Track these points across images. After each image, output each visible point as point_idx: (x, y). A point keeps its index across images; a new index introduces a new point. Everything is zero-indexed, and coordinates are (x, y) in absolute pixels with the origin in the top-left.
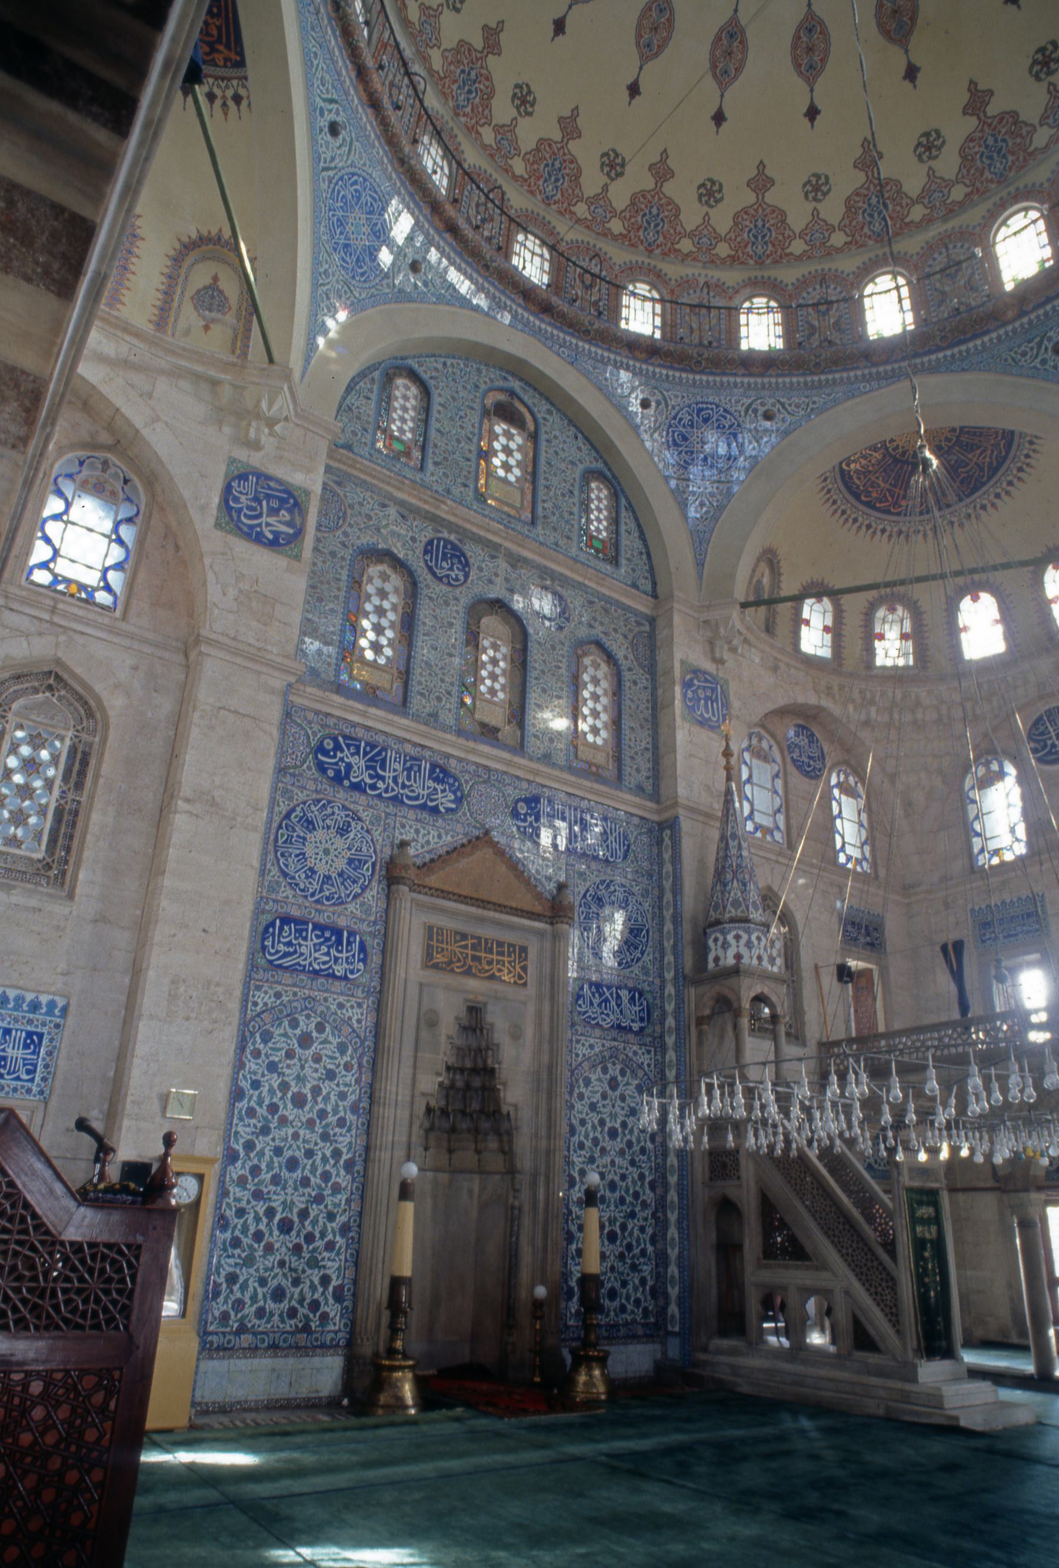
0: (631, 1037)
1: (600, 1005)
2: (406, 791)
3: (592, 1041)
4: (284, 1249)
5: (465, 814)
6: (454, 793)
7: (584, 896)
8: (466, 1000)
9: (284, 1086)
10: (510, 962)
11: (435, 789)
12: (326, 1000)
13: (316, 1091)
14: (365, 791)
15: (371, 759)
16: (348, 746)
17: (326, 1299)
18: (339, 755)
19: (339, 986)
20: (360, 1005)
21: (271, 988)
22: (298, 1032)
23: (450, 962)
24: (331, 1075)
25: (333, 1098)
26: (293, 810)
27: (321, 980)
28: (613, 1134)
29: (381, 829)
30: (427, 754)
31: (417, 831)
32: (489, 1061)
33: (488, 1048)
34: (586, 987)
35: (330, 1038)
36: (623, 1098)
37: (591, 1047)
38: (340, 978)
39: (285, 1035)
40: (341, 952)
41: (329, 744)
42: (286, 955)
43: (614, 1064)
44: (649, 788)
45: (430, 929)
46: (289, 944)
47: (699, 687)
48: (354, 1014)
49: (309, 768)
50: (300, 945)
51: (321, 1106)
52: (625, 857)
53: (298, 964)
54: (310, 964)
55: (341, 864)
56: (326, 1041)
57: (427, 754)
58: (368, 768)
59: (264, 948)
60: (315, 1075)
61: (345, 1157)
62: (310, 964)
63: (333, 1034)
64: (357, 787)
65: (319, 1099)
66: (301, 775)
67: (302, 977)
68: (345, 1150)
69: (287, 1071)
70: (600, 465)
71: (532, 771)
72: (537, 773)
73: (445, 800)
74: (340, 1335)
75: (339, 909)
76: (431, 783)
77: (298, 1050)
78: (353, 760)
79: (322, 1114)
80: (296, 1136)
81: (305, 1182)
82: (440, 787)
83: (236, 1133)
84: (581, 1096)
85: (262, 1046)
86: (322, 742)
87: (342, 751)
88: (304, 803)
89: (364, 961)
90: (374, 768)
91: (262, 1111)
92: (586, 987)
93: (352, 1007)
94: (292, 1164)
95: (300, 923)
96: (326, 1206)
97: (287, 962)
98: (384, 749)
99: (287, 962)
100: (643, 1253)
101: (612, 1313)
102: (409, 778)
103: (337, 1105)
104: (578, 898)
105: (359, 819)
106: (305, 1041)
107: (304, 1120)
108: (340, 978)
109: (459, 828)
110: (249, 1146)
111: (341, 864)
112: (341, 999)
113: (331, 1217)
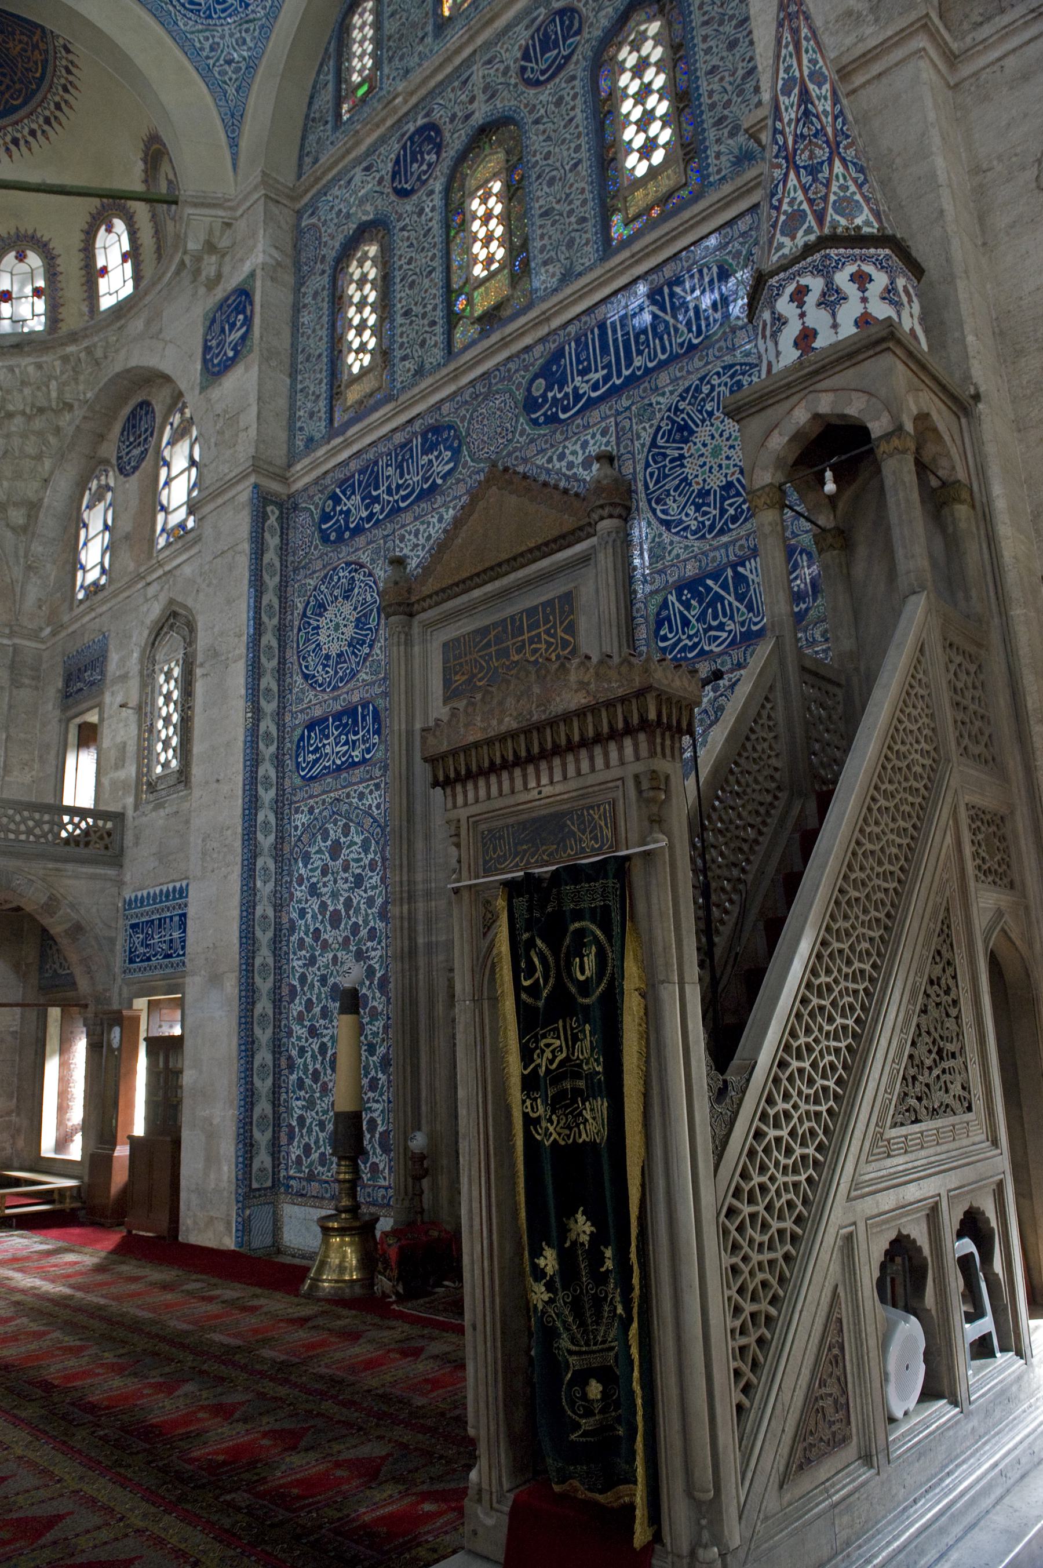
1: (701, 618)
7: (654, 444)
9: (323, 906)
10: (547, 632)
12: (348, 796)
14: (364, 529)
15: (368, 485)
16: (344, 493)
19: (358, 773)
20: (377, 786)
22: (329, 843)
25: (363, 907)
30: (417, 426)
34: (672, 598)
35: (356, 839)
38: (359, 763)
40: (356, 733)
50: (324, 745)
51: (354, 919)
53: (325, 768)
55: (349, 631)
56: (353, 843)
58: (363, 500)
59: (298, 764)
60: (346, 886)
61: (378, 975)
63: (357, 833)
64: (358, 531)
68: (377, 966)
69: (324, 890)
71: (537, 323)
75: (350, 686)
77: (331, 863)
79: (355, 929)
86: (323, 510)
89: (378, 732)
90: (369, 495)
91: (308, 940)
98: (376, 463)
99: (315, 772)
102: (402, 476)
103: (367, 915)
104: (641, 457)
105: (362, 566)
106: (335, 850)
108: (359, 763)
110: (303, 978)
111: (349, 631)
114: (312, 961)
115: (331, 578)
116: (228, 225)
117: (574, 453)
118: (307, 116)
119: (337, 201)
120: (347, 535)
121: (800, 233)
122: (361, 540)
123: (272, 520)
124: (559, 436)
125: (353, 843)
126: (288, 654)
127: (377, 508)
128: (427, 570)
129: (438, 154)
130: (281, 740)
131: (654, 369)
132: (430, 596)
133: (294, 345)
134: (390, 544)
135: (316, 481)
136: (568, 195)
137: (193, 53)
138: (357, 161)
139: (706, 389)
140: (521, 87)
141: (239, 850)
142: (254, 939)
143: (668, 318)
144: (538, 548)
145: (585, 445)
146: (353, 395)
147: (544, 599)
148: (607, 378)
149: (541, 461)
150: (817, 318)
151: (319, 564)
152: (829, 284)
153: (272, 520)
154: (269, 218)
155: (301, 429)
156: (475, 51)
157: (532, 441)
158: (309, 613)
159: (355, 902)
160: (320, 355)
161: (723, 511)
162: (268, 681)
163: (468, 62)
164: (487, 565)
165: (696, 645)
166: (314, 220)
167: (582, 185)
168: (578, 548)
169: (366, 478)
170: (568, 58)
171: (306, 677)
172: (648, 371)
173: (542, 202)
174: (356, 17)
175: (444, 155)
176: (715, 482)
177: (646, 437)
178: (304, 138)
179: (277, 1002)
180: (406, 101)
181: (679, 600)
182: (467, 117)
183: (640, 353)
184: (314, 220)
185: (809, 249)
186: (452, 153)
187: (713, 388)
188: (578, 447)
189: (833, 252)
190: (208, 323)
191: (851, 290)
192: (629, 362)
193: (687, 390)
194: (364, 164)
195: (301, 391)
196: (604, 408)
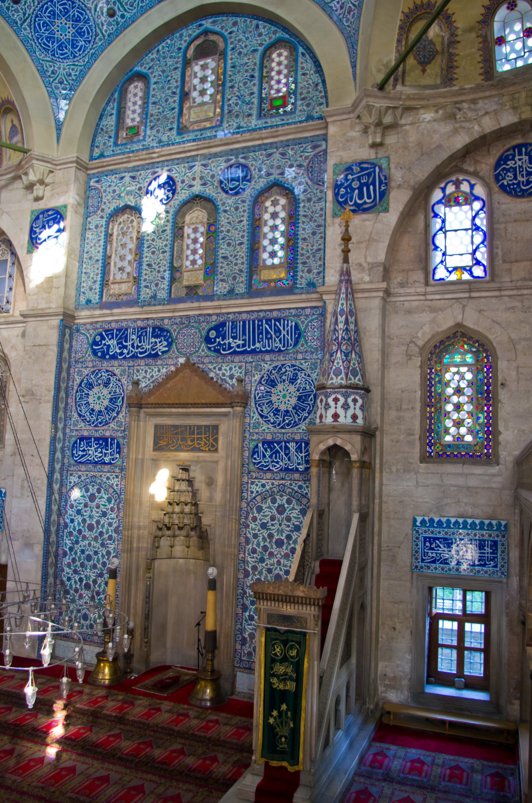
0: (296, 476)
1: (271, 457)
2: (139, 350)
3: (264, 482)
5: (174, 352)
6: (167, 340)
9: (84, 521)
10: (206, 438)
11: (156, 342)
12: (101, 476)
13: (98, 522)
15: (121, 338)
16: (107, 336)
19: (107, 468)
20: (117, 477)
23: (168, 444)
24: (104, 514)
25: (106, 526)
26: (83, 381)
27: (99, 466)
28: (279, 543)
29: (126, 377)
30: (150, 322)
31: (146, 372)
34: (260, 445)
36: (289, 519)
37: (263, 486)
40: (107, 450)
41: (98, 338)
42: (83, 456)
43: (282, 496)
45: (156, 426)
46: (84, 450)
47: (353, 180)
52: (296, 344)
55: (106, 403)
56: (102, 497)
57: (150, 322)
58: (118, 344)
59: (73, 454)
64: (114, 357)
67: (90, 466)
70: (280, 34)
71: (216, 308)
72: (220, 307)
75: (106, 427)
76: (153, 340)
77: (89, 503)
80: (90, 544)
81: (95, 567)
84: (255, 519)
86: (94, 339)
89: (119, 453)
90: (121, 343)
91: (75, 533)
94: (89, 558)
95: (88, 438)
99: (83, 460)
102: (140, 342)
105: (115, 375)
109: (170, 362)
114: (77, 542)
115: (97, 374)
116: (51, 172)
117: (226, 370)
118: (98, 125)
119: (113, 184)
120: (107, 357)
121: (339, 378)
122: (116, 363)
123: (67, 336)
124: (219, 360)
125: (102, 497)
126: (70, 401)
127: (125, 351)
128: (151, 392)
129: (173, 194)
130: (64, 440)
131: (264, 352)
133: (82, 246)
134: (131, 371)
135: (91, 323)
136: (236, 256)
137: (43, 73)
138: (128, 170)
139: (284, 370)
140: (220, 190)
142: (50, 531)
143: (272, 333)
145: (231, 369)
146: (115, 289)
148: (244, 345)
149: (211, 366)
150: (341, 412)
151: (90, 364)
152: (346, 401)
153: (67, 336)
154: (77, 179)
155: (84, 293)
156: (197, 155)
157: (207, 356)
158: (83, 385)
160: (97, 261)
161: (284, 420)
162: (61, 414)
163: (194, 158)
164: (181, 402)
166: (98, 186)
167: (243, 255)
168: (223, 410)
169: (121, 334)
171: (80, 415)
172: (261, 351)
173: (223, 251)
174: (132, 86)
175: (176, 197)
176: (283, 408)
178: (95, 136)
179: (56, 556)
181: (263, 446)
182: (191, 186)
183: (259, 342)
184: (98, 186)
185: (341, 387)
186: (181, 199)
187: (286, 371)
188: (228, 368)
189: (349, 390)
190: (34, 217)
191: (351, 404)
192: (254, 344)
193: (276, 367)
194: (131, 174)
195: (85, 273)
196: (241, 357)
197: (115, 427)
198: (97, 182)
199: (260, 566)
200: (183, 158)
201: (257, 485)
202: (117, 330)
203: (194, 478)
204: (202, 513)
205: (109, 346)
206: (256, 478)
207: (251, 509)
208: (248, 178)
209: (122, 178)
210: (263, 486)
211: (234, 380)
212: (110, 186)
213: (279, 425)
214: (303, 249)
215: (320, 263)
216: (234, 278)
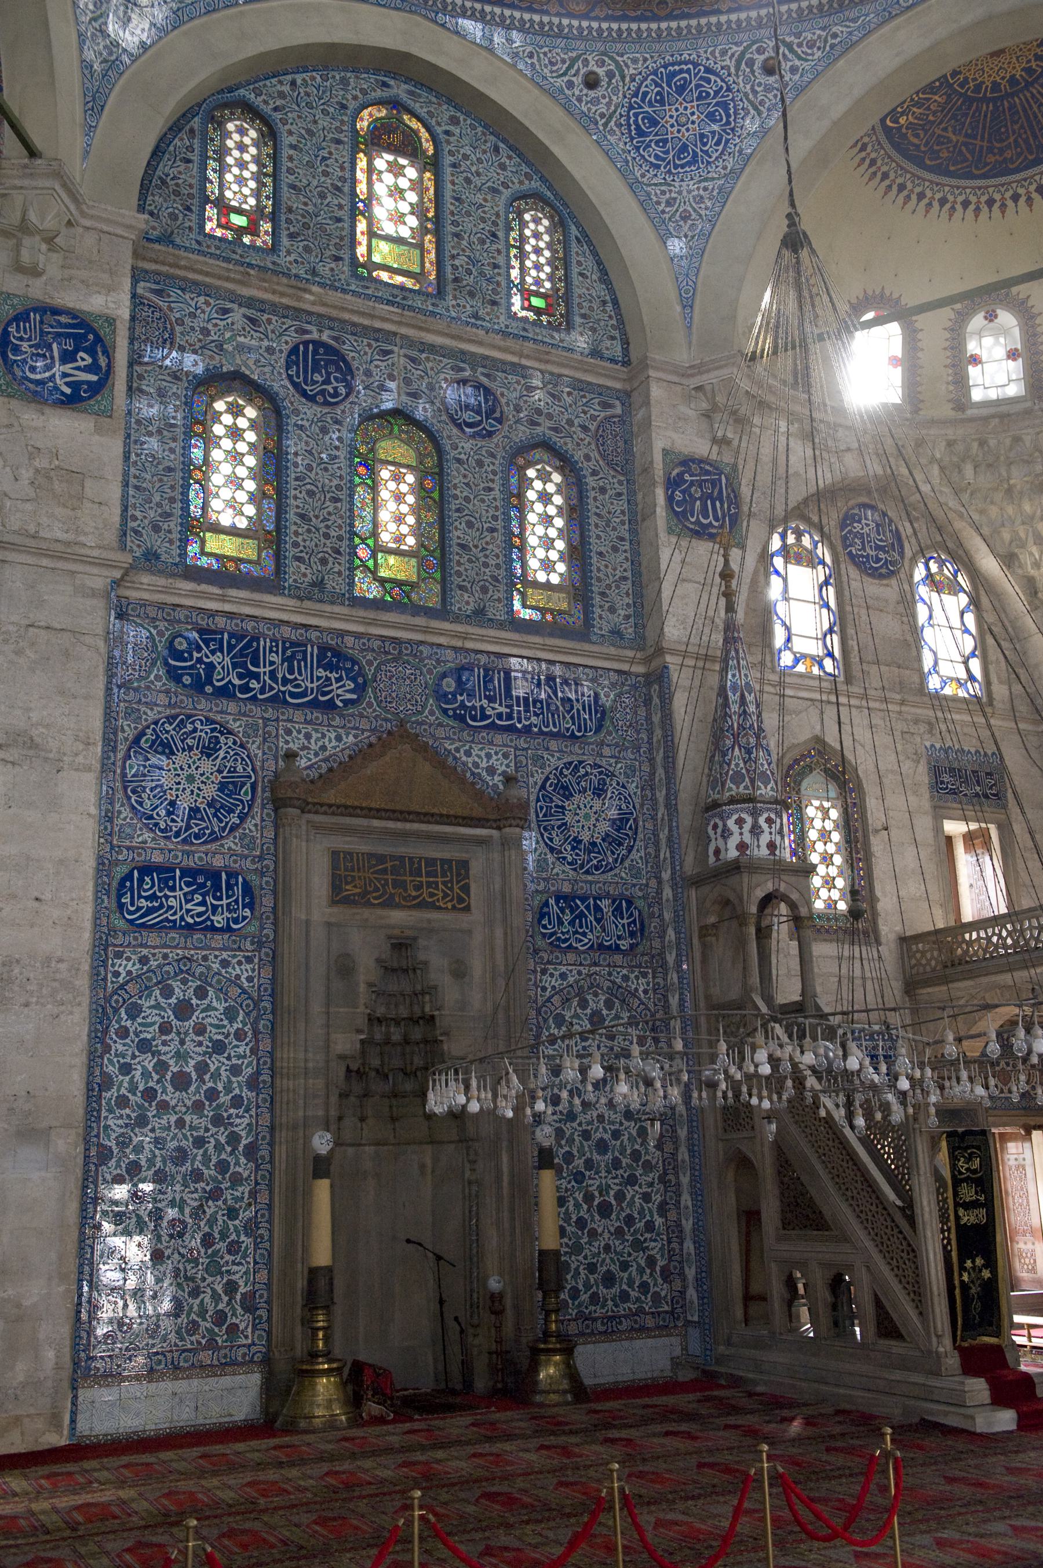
0: (618, 958)
1: (572, 923)
2: (289, 687)
3: (564, 969)
4: (176, 1256)
5: (370, 705)
6: (353, 679)
7: (543, 787)
8: (390, 937)
9: (162, 1067)
10: (444, 883)
11: (328, 679)
12: (205, 958)
13: (202, 1068)
15: (241, 654)
16: (207, 643)
17: (234, 1309)
18: (196, 655)
19: (219, 940)
20: (249, 960)
21: (135, 953)
22: (173, 1000)
23: (365, 893)
24: (219, 1047)
26: (142, 734)
27: (197, 936)
29: (259, 740)
31: (308, 736)
32: (427, 1009)
33: (423, 993)
34: (552, 901)
35: (215, 1004)
37: (563, 976)
39: (157, 1006)
42: (150, 911)
43: (596, 995)
44: (629, 631)
45: (335, 854)
46: (153, 897)
47: (692, 483)
48: (243, 972)
49: (158, 678)
50: (167, 897)
51: (210, 1084)
53: (167, 920)
54: (182, 918)
55: (210, 791)
56: (209, 1008)
57: (313, 635)
58: (235, 665)
59: (121, 906)
61: (244, 1142)
62: (182, 918)
63: (218, 999)
64: (225, 692)
65: (207, 1077)
66: (148, 688)
68: (243, 1134)
71: (456, 636)
72: (465, 637)
73: (342, 690)
74: (254, 1349)
75: (213, 847)
76: (321, 673)
78: (216, 659)
80: (180, 1123)
82: (333, 675)
83: (107, 1127)
85: (129, 1023)
87: (199, 649)
88: (156, 723)
89: (251, 906)
90: (244, 665)
92: (552, 901)
93: (240, 963)
95: (164, 873)
96: (225, 1201)
97: (151, 919)
99: (151, 919)
100: (650, 1227)
101: (610, 1303)
103: (230, 1082)
105: (230, 732)
106: (183, 1010)
107: (189, 1103)
109: (364, 724)
112: (225, 955)
113: (232, 1213)
122: (232, 707)
125: (209, 1008)
127: (254, 684)
132: (330, 806)
136: (484, 549)
141: (87, 992)
144: (448, 816)
145: (489, 756)
147: (447, 855)
148: (510, 717)
156: (395, 334)
157: (440, 725)
159: (212, 1068)
164: (398, 807)
165: (566, 940)
169: (246, 649)
170: (490, 434)
172: (541, 733)
177: (539, 778)
180: (313, 303)
181: (557, 902)
197: (238, 849)
198: (159, 293)
199: (568, 1128)
200: (365, 327)
201: (552, 975)
202: (231, 635)
203: (426, 963)
204: (446, 1034)
205: (211, 667)
206: (549, 962)
207: (545, 1020)
208: (497, 415)
209: (226, 311)
210: (563, 976)
211: (497, 778)
212: (193, 315)
213: (582, 866)
214: (599, 570)
215: (627, 600)
216: (484, 590)
